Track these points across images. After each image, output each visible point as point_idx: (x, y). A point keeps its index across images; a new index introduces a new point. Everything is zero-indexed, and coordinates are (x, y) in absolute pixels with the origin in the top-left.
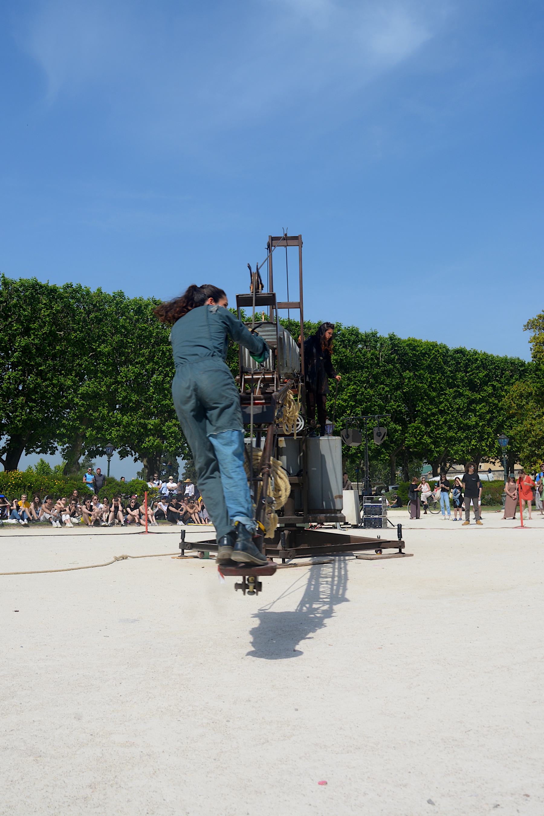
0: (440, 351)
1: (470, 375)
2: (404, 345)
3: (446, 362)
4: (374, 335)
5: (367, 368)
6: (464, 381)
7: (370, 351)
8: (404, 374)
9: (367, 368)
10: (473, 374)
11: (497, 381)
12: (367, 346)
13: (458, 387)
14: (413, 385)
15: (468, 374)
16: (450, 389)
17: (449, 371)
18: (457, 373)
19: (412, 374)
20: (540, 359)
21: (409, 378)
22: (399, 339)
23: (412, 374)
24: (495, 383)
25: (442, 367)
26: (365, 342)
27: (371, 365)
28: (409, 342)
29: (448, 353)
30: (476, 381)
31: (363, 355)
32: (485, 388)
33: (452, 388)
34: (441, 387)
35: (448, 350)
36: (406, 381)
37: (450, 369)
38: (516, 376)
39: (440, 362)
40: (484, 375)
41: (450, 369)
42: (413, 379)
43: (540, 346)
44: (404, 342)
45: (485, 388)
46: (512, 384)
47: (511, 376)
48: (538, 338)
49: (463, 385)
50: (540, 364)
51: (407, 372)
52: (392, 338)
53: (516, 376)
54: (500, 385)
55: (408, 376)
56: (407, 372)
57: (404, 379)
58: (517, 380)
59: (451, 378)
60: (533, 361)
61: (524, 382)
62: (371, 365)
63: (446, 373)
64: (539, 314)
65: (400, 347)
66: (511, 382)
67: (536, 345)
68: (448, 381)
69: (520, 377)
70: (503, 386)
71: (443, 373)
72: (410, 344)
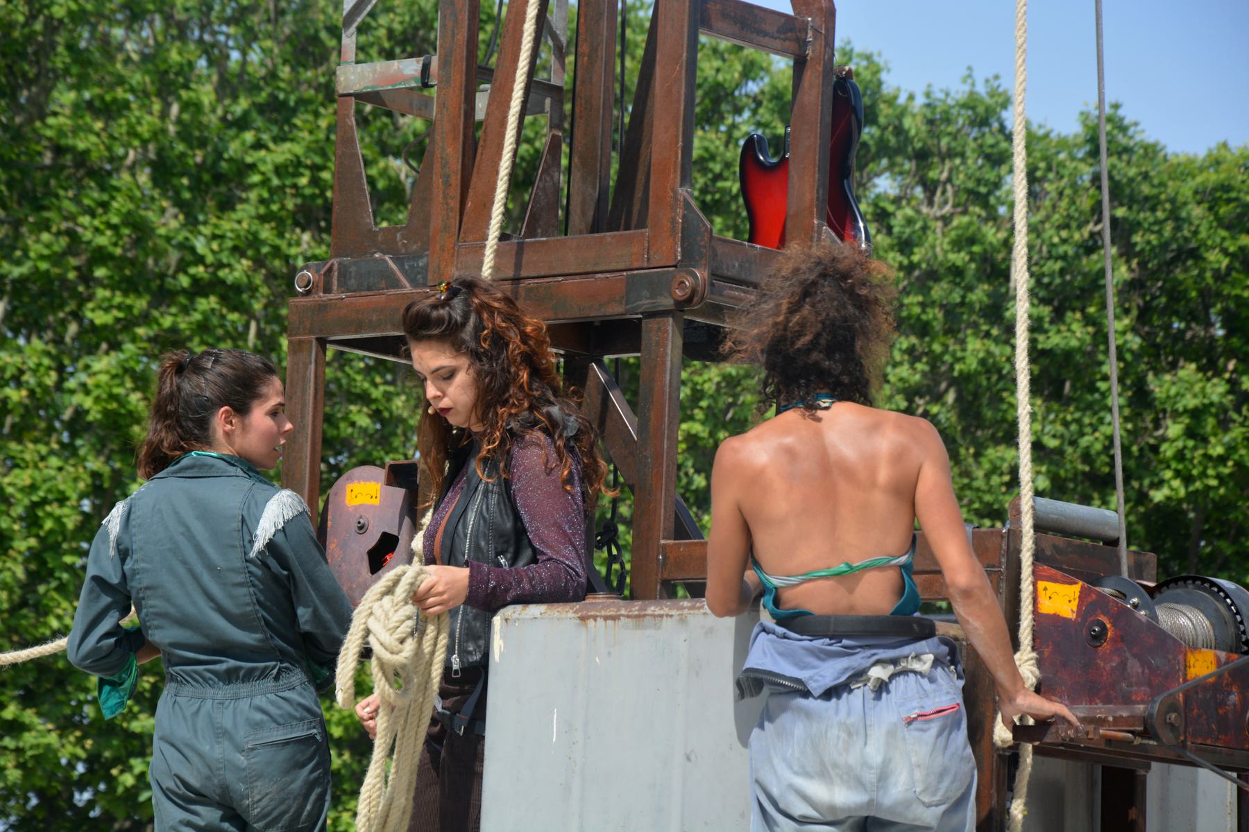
2: (1186, 190)
4: (985, 113)
5: (923, 330)
7: (946, 220)
8: (1161, 386)
9: (923, 330)
12: (930, 188)
14: (1222, 460)
19: (1217, 390)
21: (1197, 414)
22: (1151, 151)
23: (1217, 390)
26: (922, 156)
27: (951, 312)
28: (1212, 178)
31: (905, 246)
36: (1174, 429)
42: (1224, 424)
44: (1183, 171)
51: (1188, 370)
52: (1105, 137)
55: (1191, 402)
56: (1188, 370)
57: (1157, 424)
62: (951, 312)
65: (1152, 203)
72: (1226, 188)
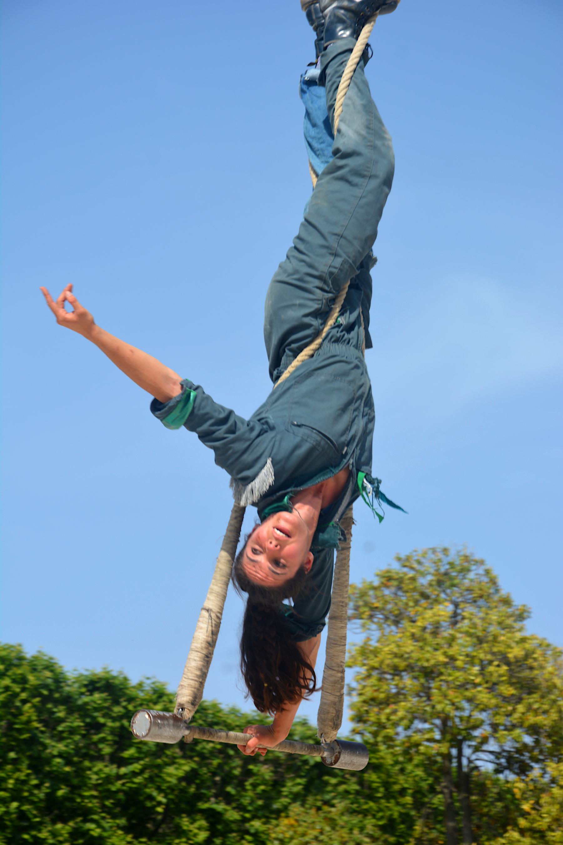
0: (32, 679)
1: (135, 774)
3: (51, 723)
6: (109, 794)
10: (142, 772)
11: (228, 799)
13: (86, 814)
15: (123, 770)
16: (54, 822)
17: (60, 755)
18: (87, 763)
20: (382, 726)
24: (220, 807)
25: (34, 741)
29: (58, 688)
30: (151, 798)
32: (185, 822)
33: (65, 821)
34: (22, 815)
35: (59, 680)
37: (61, 747)
38: (294, 785)
39: (29, 722)
40: (181, 773)
41: (61, 747)
43: (380, 680)
45: (185, 822)
46: (278, 813)
47: (277, 784)
48: (375, 652)
49: (104, 808)
50: (376, 744)
53: (294, 785)
54: (233, 815)
58: (296, 797)
59: (64, 779)
60: (354, 731)
61: (319, 809)
63: (48, 761)
64: (384, 568)
66: (276, 806)
67: (369, 676)
68: (51, 796)
69: (307, 788)
70: (245, 820)
71: (38, 764)
